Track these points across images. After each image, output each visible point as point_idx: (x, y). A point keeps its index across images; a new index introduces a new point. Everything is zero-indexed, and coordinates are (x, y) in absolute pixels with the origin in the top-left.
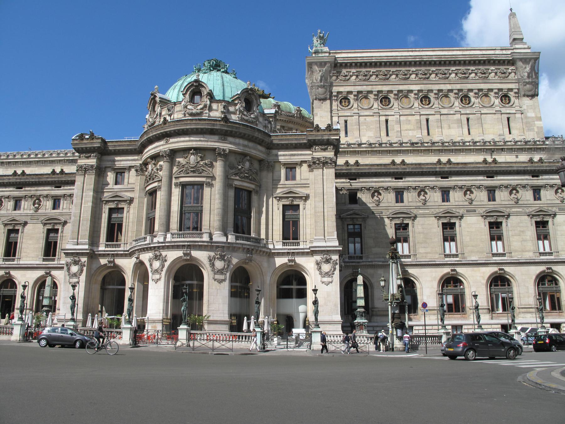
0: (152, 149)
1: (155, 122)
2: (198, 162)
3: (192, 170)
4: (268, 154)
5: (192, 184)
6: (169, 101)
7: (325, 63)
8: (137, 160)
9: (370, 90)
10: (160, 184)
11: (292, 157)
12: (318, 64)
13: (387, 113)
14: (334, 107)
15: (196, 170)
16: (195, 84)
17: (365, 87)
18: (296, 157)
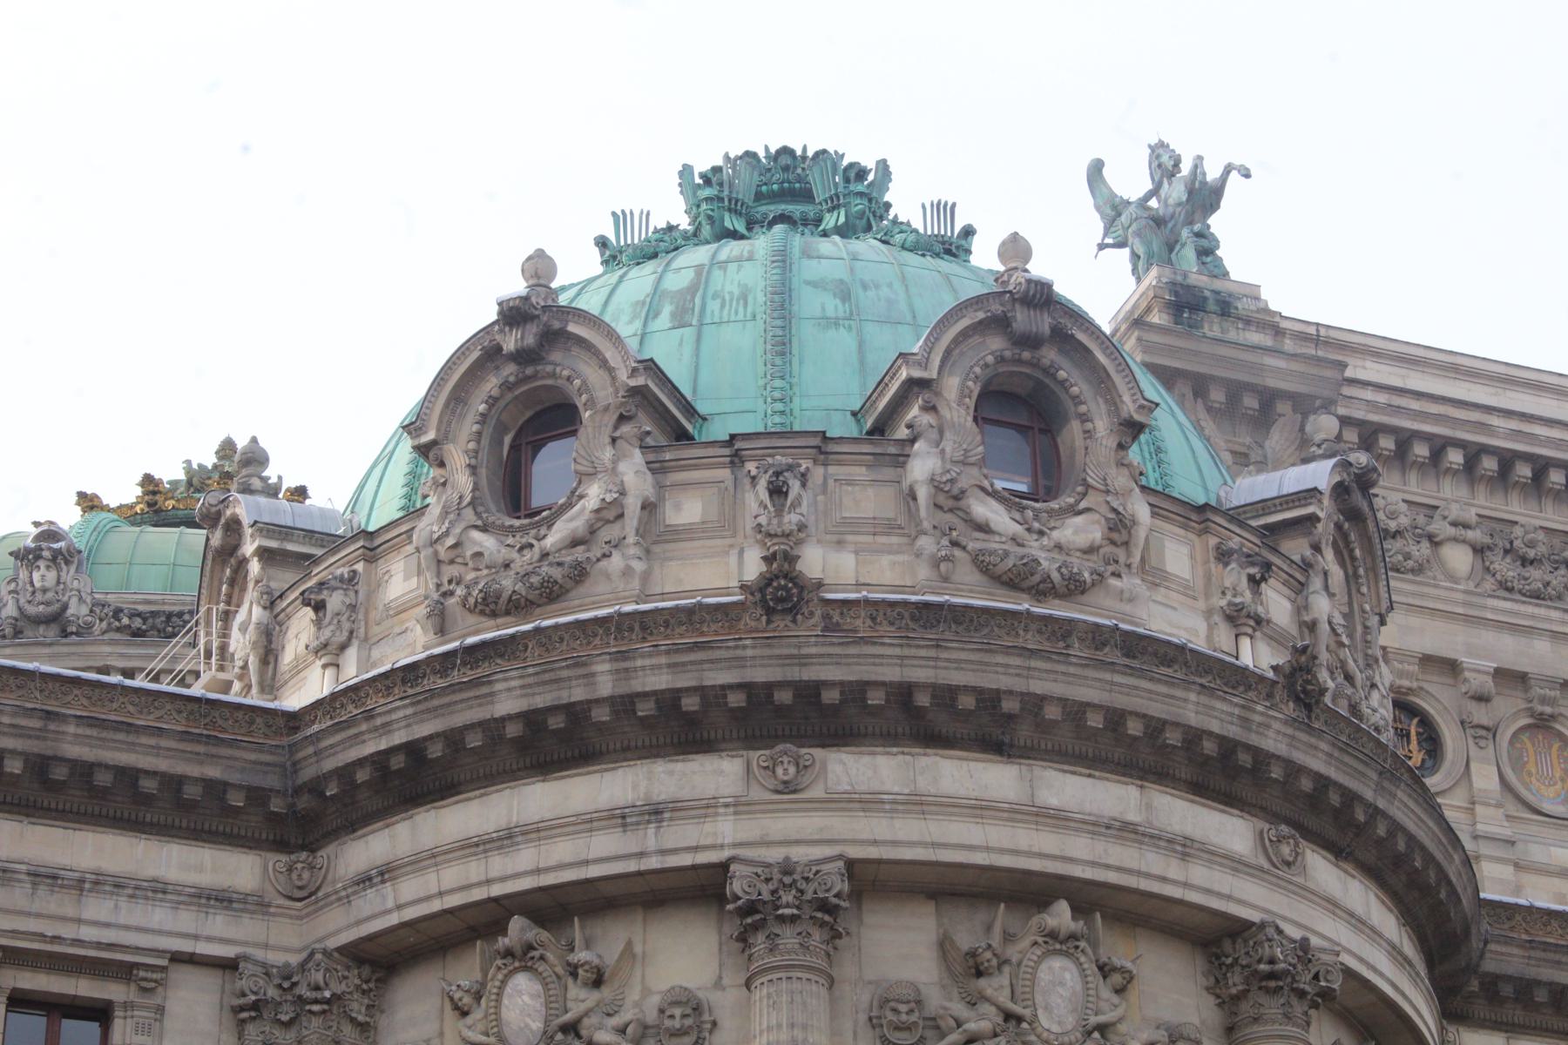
0: (588, 822)
1: (580, 573)
6: (690, 410)
7: (1269, 398)
8: (255, 904)
12: (1218, 396)
16: (1022, 319)
17: (1542, 646)
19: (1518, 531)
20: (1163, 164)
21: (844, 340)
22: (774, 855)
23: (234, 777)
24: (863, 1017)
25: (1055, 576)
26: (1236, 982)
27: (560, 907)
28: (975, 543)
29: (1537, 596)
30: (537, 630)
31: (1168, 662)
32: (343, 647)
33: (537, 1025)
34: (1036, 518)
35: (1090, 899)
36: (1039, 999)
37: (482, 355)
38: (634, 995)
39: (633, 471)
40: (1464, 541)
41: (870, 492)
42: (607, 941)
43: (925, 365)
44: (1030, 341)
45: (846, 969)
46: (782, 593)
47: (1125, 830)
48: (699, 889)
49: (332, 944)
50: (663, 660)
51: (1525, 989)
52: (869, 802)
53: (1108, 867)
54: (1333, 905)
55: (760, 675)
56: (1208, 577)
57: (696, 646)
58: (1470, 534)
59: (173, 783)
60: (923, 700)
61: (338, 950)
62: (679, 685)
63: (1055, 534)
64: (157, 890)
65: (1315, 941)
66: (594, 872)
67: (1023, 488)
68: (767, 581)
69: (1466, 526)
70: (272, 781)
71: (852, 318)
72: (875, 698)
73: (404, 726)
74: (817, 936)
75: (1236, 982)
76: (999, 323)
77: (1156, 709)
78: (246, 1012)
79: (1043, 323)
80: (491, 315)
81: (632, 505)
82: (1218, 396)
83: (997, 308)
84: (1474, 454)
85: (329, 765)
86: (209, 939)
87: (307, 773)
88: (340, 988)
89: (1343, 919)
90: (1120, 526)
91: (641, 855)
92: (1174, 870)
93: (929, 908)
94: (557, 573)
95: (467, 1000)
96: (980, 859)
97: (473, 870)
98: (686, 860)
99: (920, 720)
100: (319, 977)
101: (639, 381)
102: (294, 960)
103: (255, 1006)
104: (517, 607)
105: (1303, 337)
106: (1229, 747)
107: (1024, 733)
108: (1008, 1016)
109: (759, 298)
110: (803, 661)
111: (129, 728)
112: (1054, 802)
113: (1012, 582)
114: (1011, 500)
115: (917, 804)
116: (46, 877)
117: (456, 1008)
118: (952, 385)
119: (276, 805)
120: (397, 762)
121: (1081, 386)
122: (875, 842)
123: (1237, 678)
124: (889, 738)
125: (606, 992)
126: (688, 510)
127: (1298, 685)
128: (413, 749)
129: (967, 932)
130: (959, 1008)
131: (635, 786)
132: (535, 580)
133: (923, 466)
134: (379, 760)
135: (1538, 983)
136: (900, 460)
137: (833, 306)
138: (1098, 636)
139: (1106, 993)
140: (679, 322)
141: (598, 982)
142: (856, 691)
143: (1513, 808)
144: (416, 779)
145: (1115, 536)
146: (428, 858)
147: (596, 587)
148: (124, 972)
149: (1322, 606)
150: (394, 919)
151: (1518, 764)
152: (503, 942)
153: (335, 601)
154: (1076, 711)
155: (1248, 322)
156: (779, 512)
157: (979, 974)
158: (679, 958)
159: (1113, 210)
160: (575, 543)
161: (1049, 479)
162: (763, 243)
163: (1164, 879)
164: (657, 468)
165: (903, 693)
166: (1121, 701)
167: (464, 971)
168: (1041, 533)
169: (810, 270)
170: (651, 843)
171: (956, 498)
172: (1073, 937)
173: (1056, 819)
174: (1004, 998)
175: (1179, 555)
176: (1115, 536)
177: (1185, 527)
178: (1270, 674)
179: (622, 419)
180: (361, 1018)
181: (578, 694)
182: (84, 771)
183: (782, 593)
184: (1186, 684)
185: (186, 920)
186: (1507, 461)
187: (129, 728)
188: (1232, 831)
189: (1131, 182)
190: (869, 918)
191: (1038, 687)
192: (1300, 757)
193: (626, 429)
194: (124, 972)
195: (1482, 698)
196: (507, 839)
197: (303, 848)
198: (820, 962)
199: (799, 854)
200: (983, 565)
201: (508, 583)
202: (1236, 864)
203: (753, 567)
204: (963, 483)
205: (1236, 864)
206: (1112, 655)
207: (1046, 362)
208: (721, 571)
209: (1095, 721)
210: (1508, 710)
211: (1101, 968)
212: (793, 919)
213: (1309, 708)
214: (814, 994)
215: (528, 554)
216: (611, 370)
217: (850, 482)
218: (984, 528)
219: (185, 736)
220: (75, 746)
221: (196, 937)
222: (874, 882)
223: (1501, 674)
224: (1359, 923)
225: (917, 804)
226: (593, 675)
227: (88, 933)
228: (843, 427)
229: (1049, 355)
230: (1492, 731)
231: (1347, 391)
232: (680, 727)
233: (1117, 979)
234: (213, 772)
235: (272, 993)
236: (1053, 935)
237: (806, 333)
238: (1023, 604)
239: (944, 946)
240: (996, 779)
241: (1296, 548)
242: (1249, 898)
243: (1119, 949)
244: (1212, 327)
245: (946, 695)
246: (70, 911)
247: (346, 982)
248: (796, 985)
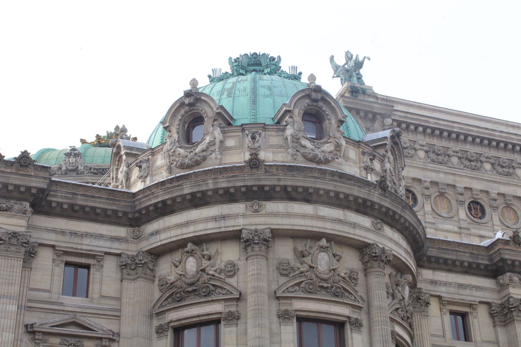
0: (207, 220)
1: (204, 159)
3: (325, 285)
5: (319, 321)
6: (232, 118)
7: (375, 115)
9: (451, 182)
10: (233, 309)
11: (462, 292)
12: (362, 114)
13: (483, 233)
15: (334, 288)
16: (314, 95)
17: (442, 175)
18: (468, 292)
19: (436, 147)
20: (349, 57)
21: (270, 100)
22: (253, 228)
23: (120, 209)
24: (275, 267)
25: (322, 159)
26: (367, 258)
27: (200, 241)
28: (302, 150)
29: (441, 163)
30: (194, 172)
31: (350, 180)
32: (146, 177)
33: (195, 270)
34: (317, 144)
35: (332, 238)
36: (318, 262)
37: (180, 105)
38: (218, 262)
39: (218, 133)
40: (423, 150)
41: (276, 138)
42: (212, 249)
43: (290, 106)
44: (316, 101)
45: (271, 256)
46: (255, 163)
47: (339, 221)
48: (235, 236)
49: (144, 250)
50: (225, 180)
51: (437, 259)
52: (276, 215)
53: (335, 230)
54: (390, 239)
55: (249, 183)
56: (360, 158)
57: (233, 176)
58: (424, 148)
59: (105, 210)
60: (289, 189)
61: (146, 251)
62: (229, 186)
63: (322, 148)
64: (101, 237)
65: (386, 248)
66: (209, 232)
67: (314, 137)
68: (251, 160)
69: (423, 146)
70: (129, 210)
71: (272, 95)
72: (278, 189)
73: (161, 196)
74: (264, 247)
75: (367, 258)
76: (308, 96)
77: (347, 191)
78: (123, 266)
79: (319, 96)
80: (182, 94)
81: (217, 141)
82: (362, 114)
83: (307, 92)
84: (425, 128)
85: (143, 206)
86: (114, 249)
87: (138, 208)
88: (146, 261)
89: (393, 242)
90: (338, 146)
91: (220, 228)
92: (351, 231)
93: (291, 240)
94: (199, 158)
95: (177, 263)
96: (304, 228)
97: (179, 231)
98: (231, 229)
99: (289, 195)
100: (141, 258)
101: (219, 111)
102: (135, 254)
103: (125, 265)
104: (189, 167)
105: (383, 99)
106: (365, 201)
107: (315, 197)
108: (311, 267)
109: (248, 90)
110: (260, 180)
111: (93, 197)
112: (322, 214)
113: (312, 160)
114: (311, 140)
115: (289, 215)
116: (74, 234)
117: (175, 265)
118: (296, 112)
119: (130, 216)
120: (160, 205)
121: (328, 112)
122: (278, 224)
123: (367, 184)
124: (281, 199)
125: (212, 261)
126: (230, 143)
127: (382, 185)
128: (164, 202)
129: (301, 246)
130: (299, 265)
131: (218, 211)
132: (193, 160)
133: (289, 131)
134: (155, 205)
135: (440, 258)
136: (284, 130)
137: (267, 92)
138: (333, 174)
139: (335, 261)
140: (229, 96)
141: (210, 259)
142: (273, 188)
143: (435, 215)
144: (164, 209)
145: (337, 149)
146: (167, 229)
147: (208, 162)
148: (93, 257)
149: (388, 166)
150: (159, 244)
151: (436, 205)
152: (186, 249)
153: (144, 165)
154: (327, 192)
155: (370, 96)
156: (254, 143)
157: (304, 257)
158: (230, 253)
159: (336, 68)
160: (203, 151)
161: (321, 135)
162: (249, 76)
163: (349, 233)
164: (223, 132)
165: (285, 188)
166: (338, 189)
167: (177, 256)
168: (319, 148)
169: (261, 83)
170: (223, 225)
171: (298, 139)
172: (327, 247)
173: (323, 218)
174: (309, 262)
175: (353, 153)
176: (337, 149)
177: (354, 147)
178: (375, 183)
179: (215, 120)
180: (151, 268)
181: (204, 188)
182: (83, 207)
183: (255, 163)
184: (355, 185)
185: (108, 244)
186: (433, 130)
187: (93, 197)
188: (366, 221)
189: (341, 61)
190: (276, 243)
191: (318, 186)
192: (383, 203)
193: (216, 123)
194: (93, 257)
195: (427, 188)
196: (187, 224)
197: (137, 226)
198: (265, 254)
199: (259, 227)
200: (304, 156)
201: (187, 161)
202: (367, 229)
203: (248, 157)
204: (299, 136)
205: (367, 229)
206: (337, 178)
207: (320, 106)
208: (239, 158)
209: (332, 194)
210: (433, 191)
211: (333, 255)
212: (258, 243)
213: (384, 191)
214: (263, 262)
215: (192, 154)
216: (212, 108)
217: (271, 136)
218: (304, 147)
219: (107, 199)
220: (80, 201)
221: (111, 248)
222: (277, 234)
223: (432, 182)
224: (397, 244)
225: (289, 215)
226: (208, 183)
227: (84, 247)
228: (269, 122)
229: (320, 104)
230: (430, 196)
231: (394, 113)
232: (229, 196)
233: (337, 257)
234: (114, 208)
235: (130, 262)
236: (322, 247)
237: (261, 99)
238: (314, 166)
239: (295, 250)
240: (308, 209)
241: (382, 151)
242: (370, 238)
243: (337, 250)
244: (361, 97)
245: (295, 188)
246: (80, 242)
247: (147, 259)
248: (259, 260)
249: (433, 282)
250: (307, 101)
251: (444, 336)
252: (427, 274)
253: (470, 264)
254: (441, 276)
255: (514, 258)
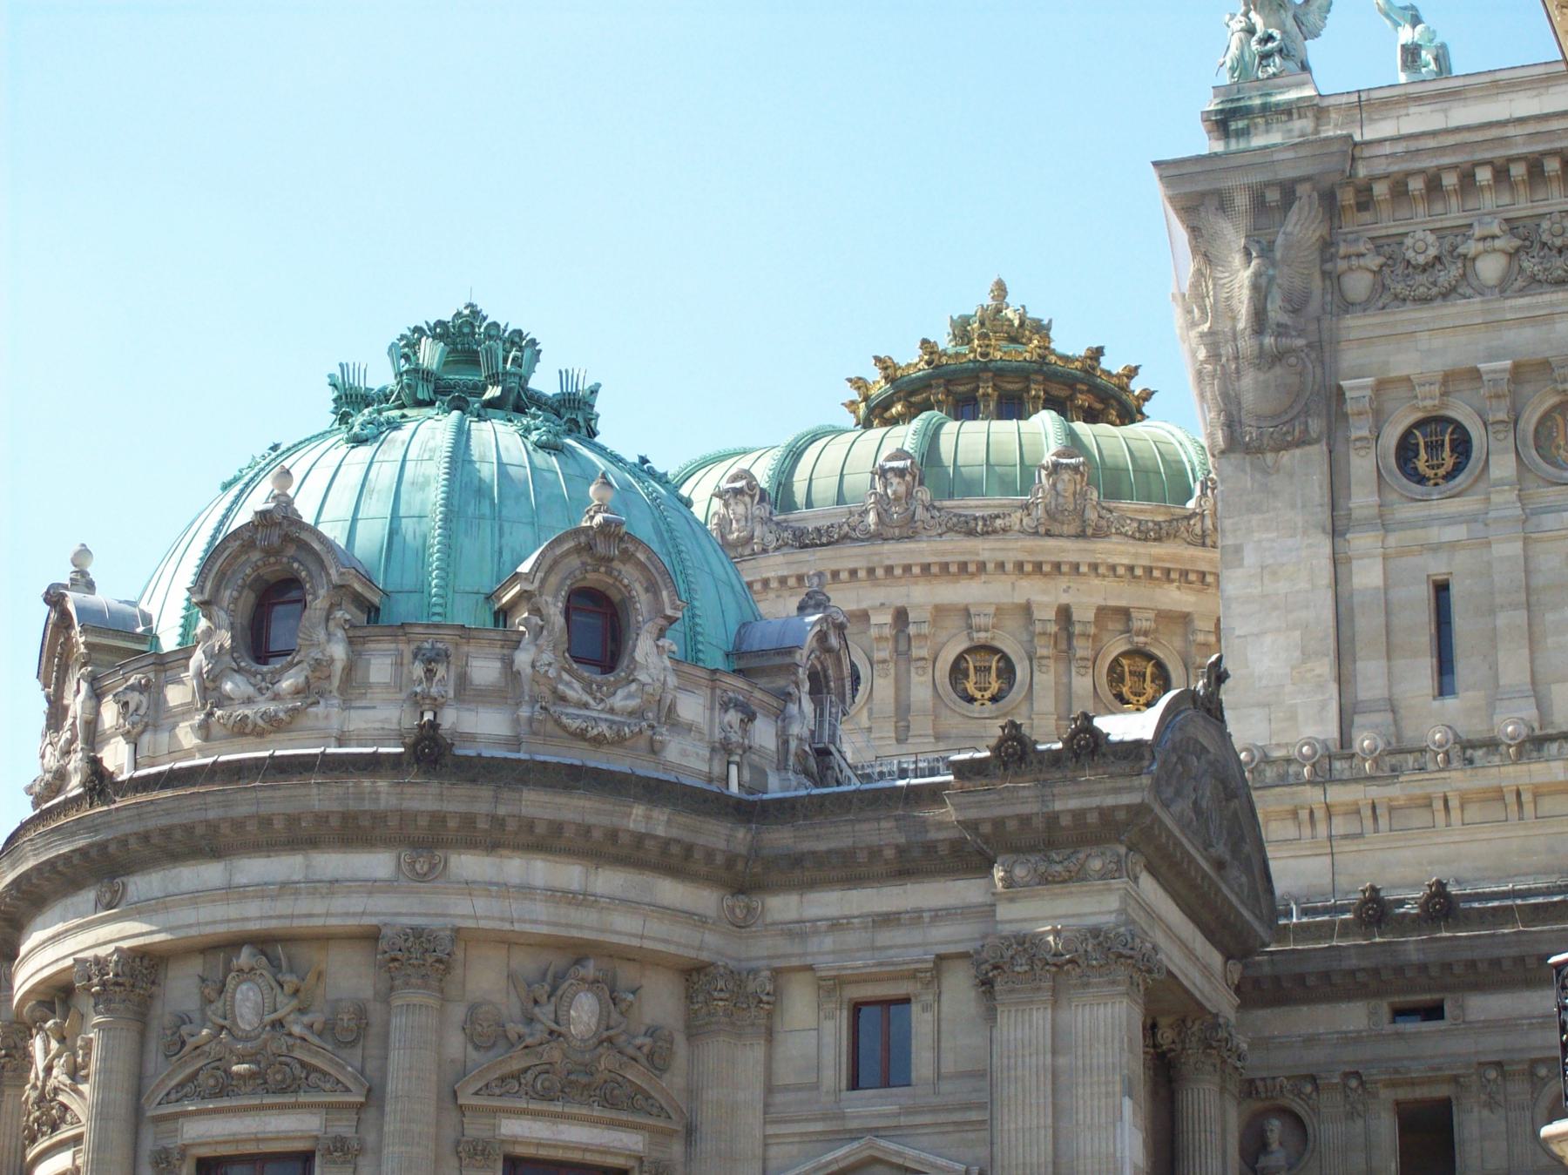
2: (278, 1024)
4: (741, 925)
7: (1289, 190)
11: (885, 937)
14: (1362, 499)
34: (264, 679)
40: (1494, 250)
47: (286, 888)
53: (271, 917)
54: (469, 887)
58: (1498, 244)
69: (1494, 237)
92: (319, 906)
163: (310, 916)
166: (265, 810)
188: (378, 863)
199: (102, 952)
240: (210, 873)
249: (797, 931)
250: (255, 556)
251: (816, 1086)
252: (782, 906)
253: (901, 851)
254: (828, 903)
255: (998, 812)
